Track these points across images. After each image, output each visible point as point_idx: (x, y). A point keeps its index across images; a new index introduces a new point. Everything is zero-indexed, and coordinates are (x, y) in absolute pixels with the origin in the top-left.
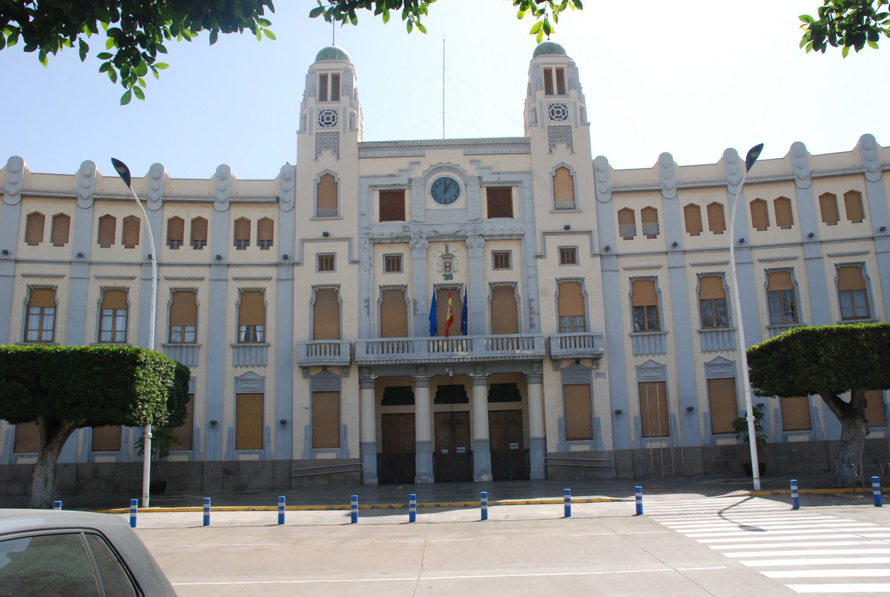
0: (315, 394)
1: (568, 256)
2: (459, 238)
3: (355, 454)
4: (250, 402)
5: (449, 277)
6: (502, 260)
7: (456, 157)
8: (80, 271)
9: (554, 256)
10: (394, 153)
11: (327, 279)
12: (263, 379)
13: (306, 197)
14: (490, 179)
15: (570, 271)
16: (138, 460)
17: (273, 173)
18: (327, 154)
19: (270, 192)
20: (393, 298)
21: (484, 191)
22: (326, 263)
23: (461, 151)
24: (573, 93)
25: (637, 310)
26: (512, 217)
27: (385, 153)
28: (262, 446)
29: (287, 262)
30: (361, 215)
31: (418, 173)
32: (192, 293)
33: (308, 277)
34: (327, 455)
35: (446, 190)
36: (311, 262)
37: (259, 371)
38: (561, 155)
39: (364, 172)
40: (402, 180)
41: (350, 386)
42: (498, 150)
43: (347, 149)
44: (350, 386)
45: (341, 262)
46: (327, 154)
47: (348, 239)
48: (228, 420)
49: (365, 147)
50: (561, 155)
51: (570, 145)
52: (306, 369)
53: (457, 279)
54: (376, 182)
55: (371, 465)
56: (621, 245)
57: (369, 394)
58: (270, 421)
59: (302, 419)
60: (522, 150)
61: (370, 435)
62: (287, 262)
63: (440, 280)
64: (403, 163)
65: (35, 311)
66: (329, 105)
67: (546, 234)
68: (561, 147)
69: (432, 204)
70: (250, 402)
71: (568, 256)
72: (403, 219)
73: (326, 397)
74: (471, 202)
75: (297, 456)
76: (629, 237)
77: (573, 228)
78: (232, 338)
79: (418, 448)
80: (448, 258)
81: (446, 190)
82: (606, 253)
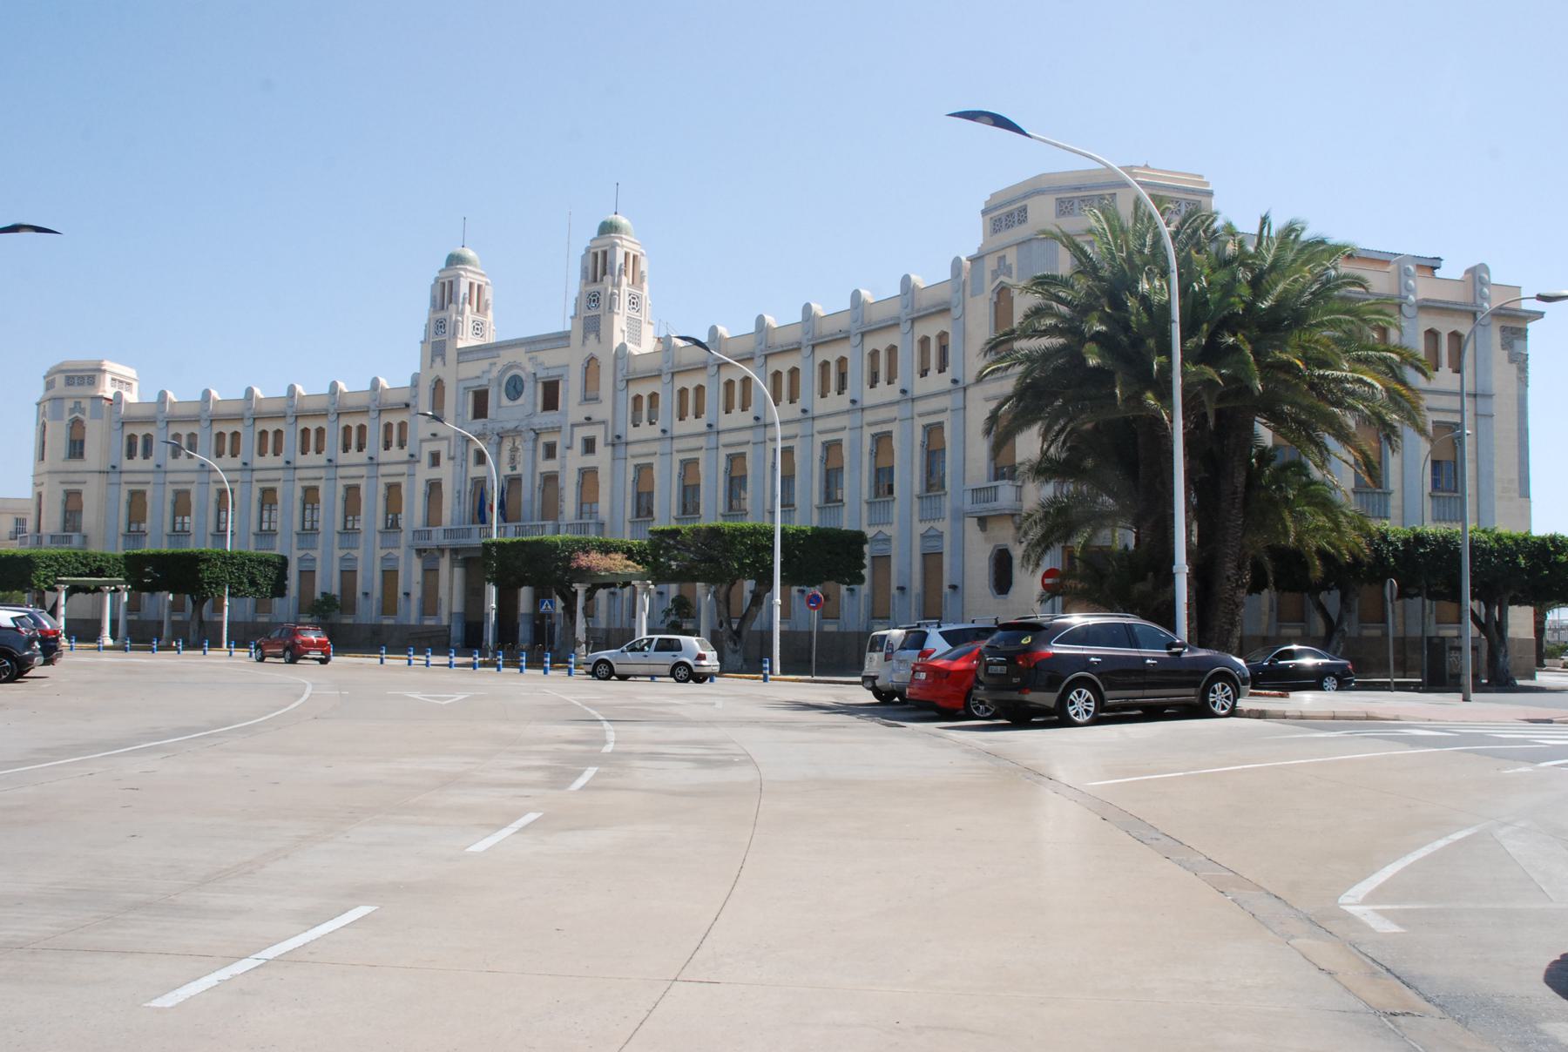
0: (426, 571)
1: (589, 446)
2: (516, 432)
3: (445, 622)
4: (390, 576)
5: (514, 468)
6: (550, 451)
7: (519, 356)
8: (289, 474)
9: (578, 446)
10: (481, 355)
11: (434, 474)
12: (397, 559)
13: (424, 404)
14: (541, 374)
15: (590, 461)
16: (765, 627)
17: (407, 382)
18: (438, 360)
19: (405, 398)
20: (480, 485)
21: (540, 387)
22: (435, 459)
23: (523, 350)
24: (608, 278)
25: (639, 496)
26: (556, 408)
27: (475, 356)
28: (395, 613)
29: (413, 459)
30: (457, 415)
31: (495, 373)
32: (357, 488)
33: (424, 472)
34: (429, 622)
35: (514, 388)
36: (426, 459)
37: (396, 552)
38: (592, 346)
39: (462, 376)
40: (484, 382)
41: (445, 564)
42: (549, 345)
43: (451, 356)
44: (445, 564)
45: (443, 459)
46: (438, 360)
47: (447, 438)
48: (377, 592)
49: (463, 353)
50: (592, 346)
51: (598, 336)
52: (420, 552)
53: (519, 470)
54: (468, 384)
55: (457, 632)
56: (633, 434)
57: (458, 572)
58: (400, 595)
59: (416, 592)
60: (560, 343)
61: (457, 607)
62: (413, 459)
63: (507, 471)
64: (485, 364)
65: (266, 507)
66: (441, 315)
67: (573, 426)
68: (592, 337)
69: (505, 401)
70: (390, 576)
71: (589, 446)
72: (485, 416)
73: (430, 572)
74: (533, 395)
75: (413, 622)
76: (635, 425)
77: (595, 418)
78: (380, 525)
79: (520, 620)
80: (514, 450)
81: (514, 388)
82: (617, 442)
